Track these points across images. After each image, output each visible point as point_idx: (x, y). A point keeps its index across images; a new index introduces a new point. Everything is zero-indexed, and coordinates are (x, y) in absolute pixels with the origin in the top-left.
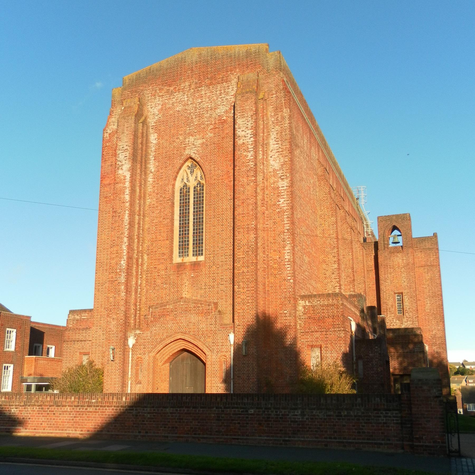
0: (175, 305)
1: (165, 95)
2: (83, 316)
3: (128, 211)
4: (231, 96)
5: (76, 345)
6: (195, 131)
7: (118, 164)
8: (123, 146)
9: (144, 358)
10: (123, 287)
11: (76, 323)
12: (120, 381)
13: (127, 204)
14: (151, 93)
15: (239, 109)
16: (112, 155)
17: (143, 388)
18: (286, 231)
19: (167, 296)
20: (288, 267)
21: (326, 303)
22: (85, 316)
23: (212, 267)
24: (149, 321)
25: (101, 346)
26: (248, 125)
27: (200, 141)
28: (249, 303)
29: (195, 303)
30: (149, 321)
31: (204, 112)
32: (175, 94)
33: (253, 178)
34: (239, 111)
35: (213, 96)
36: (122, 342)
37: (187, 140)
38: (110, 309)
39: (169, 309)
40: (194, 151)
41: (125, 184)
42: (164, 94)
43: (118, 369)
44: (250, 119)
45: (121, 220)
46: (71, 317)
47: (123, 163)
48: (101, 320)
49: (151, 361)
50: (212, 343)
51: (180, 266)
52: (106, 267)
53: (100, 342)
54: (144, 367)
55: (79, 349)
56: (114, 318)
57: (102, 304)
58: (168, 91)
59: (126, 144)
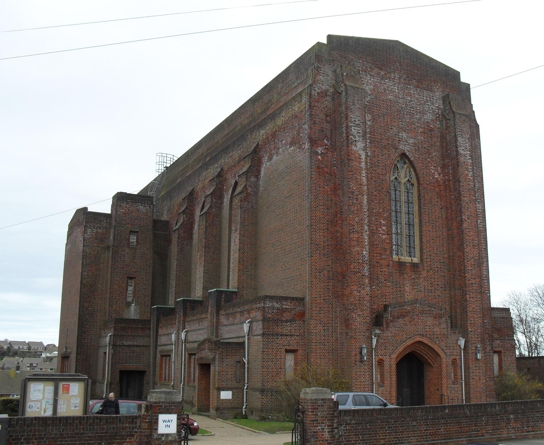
0: (412, 307)
1: (376, 77)
2: (284, 305)
3: (367, 196)
4: (436, 107)
5: (280, 340)
6: (408, 128)
7: (351, 138)
8: (354, 119)
9: (386, 360)
10: (367, 281)
11: (276, 313)
12: (370, 384)
13: (365, 188)
14: (362, 68)
15: (458, 128)
16: (323, 120)
17: (386, 392)
18: (483, 250)
19: (391, 294)
20: (486, 282)
21: (501, 316)
22: (286, 305)
23: (429, 271)
24: (389, 321)
25: (322, 344)
26: (466, 146)
27: (412, 141)
28: (478, 312)
29: (429, 307)
30: (389, 321)
31: (414, 112)
32: (386, 80)
33: (474, 198)
34: (459, 130)
35: (420, 99)
36: (369, 342)
37: (401, 134)
38: (354, 303)
39: (407, 310)
40: (407, 149)
41: (360, 164)
42: (375, 75)
43: (367, 371)
44: (467, 141)
45: (359, 204)
46: (269, 304)
47: (357, 139)
48: (321, 314)
49: (393, 363)
50: (445, 347)
51: (401, 265)
52: (323, 251)
53: (322, 339)
54: (386, 369)
55: (283, 345)
56: (359, 315)
57: (321, 295)
58: (378, 74)
59: (359, 118)
